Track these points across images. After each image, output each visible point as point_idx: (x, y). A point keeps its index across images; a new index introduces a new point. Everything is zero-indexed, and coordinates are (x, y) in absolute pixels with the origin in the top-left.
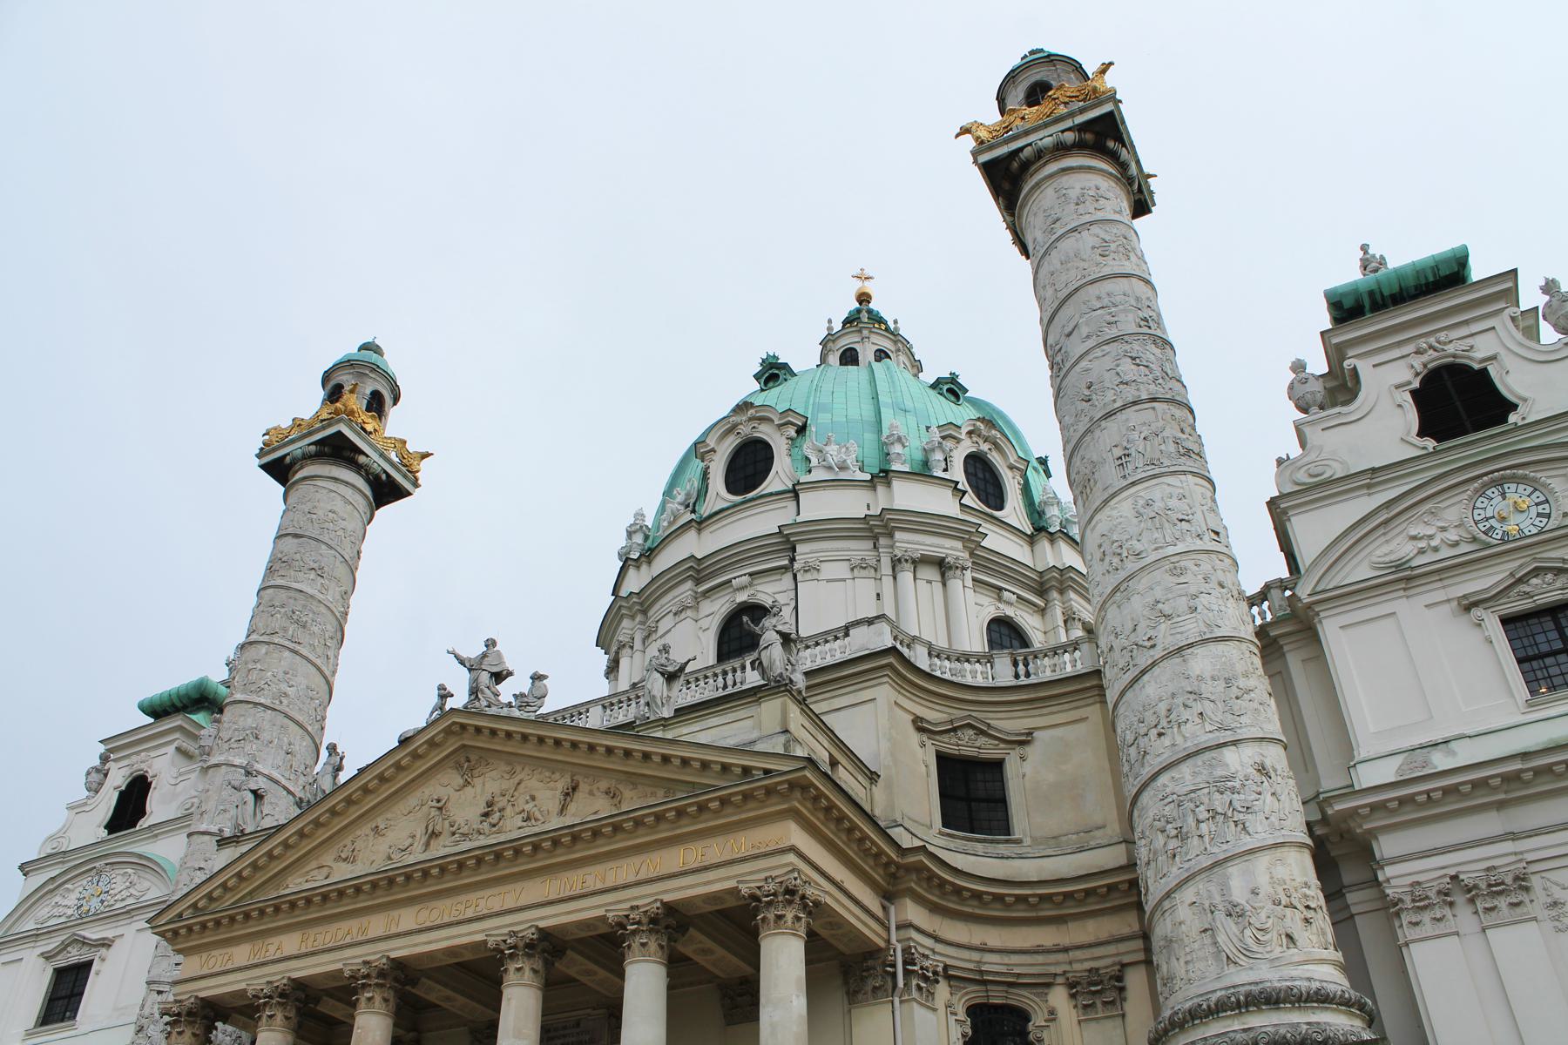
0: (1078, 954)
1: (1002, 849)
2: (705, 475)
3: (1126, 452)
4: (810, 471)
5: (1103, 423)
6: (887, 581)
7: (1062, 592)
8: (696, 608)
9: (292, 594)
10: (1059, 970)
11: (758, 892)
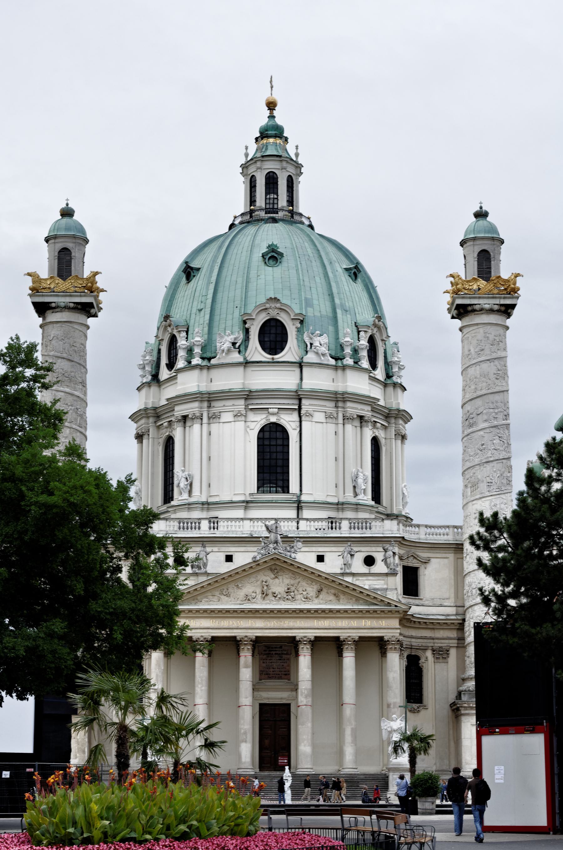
0: (436, 641)
1: (417, 602)
2: (247, 331)
3: (491, 481)
4: (307, 352)
5: (485, 465)
6: (341, 426)
7: (396, 418)
8: (245, 416)
9: (75, 398)
10: (432, 645)
11: (390, 640)
